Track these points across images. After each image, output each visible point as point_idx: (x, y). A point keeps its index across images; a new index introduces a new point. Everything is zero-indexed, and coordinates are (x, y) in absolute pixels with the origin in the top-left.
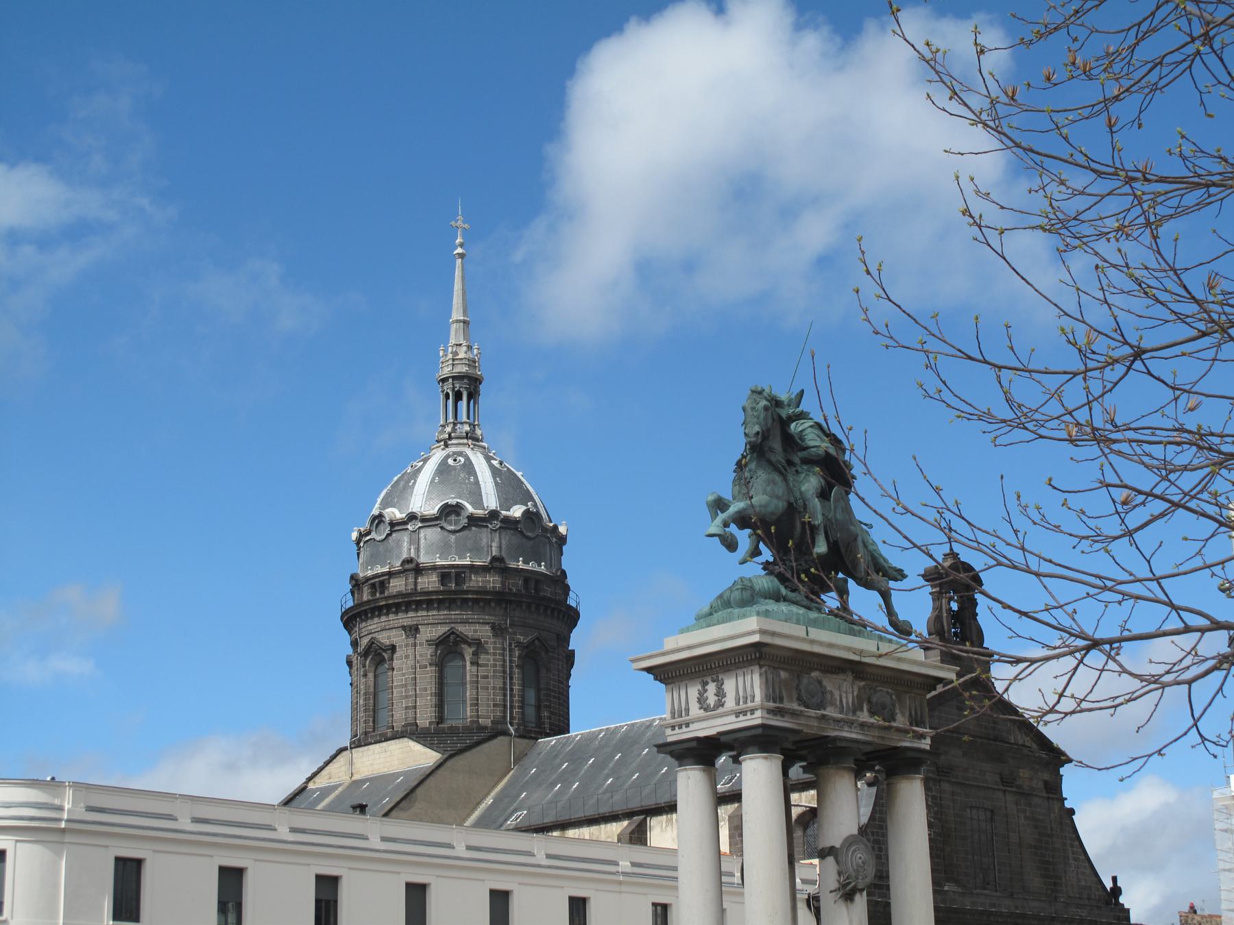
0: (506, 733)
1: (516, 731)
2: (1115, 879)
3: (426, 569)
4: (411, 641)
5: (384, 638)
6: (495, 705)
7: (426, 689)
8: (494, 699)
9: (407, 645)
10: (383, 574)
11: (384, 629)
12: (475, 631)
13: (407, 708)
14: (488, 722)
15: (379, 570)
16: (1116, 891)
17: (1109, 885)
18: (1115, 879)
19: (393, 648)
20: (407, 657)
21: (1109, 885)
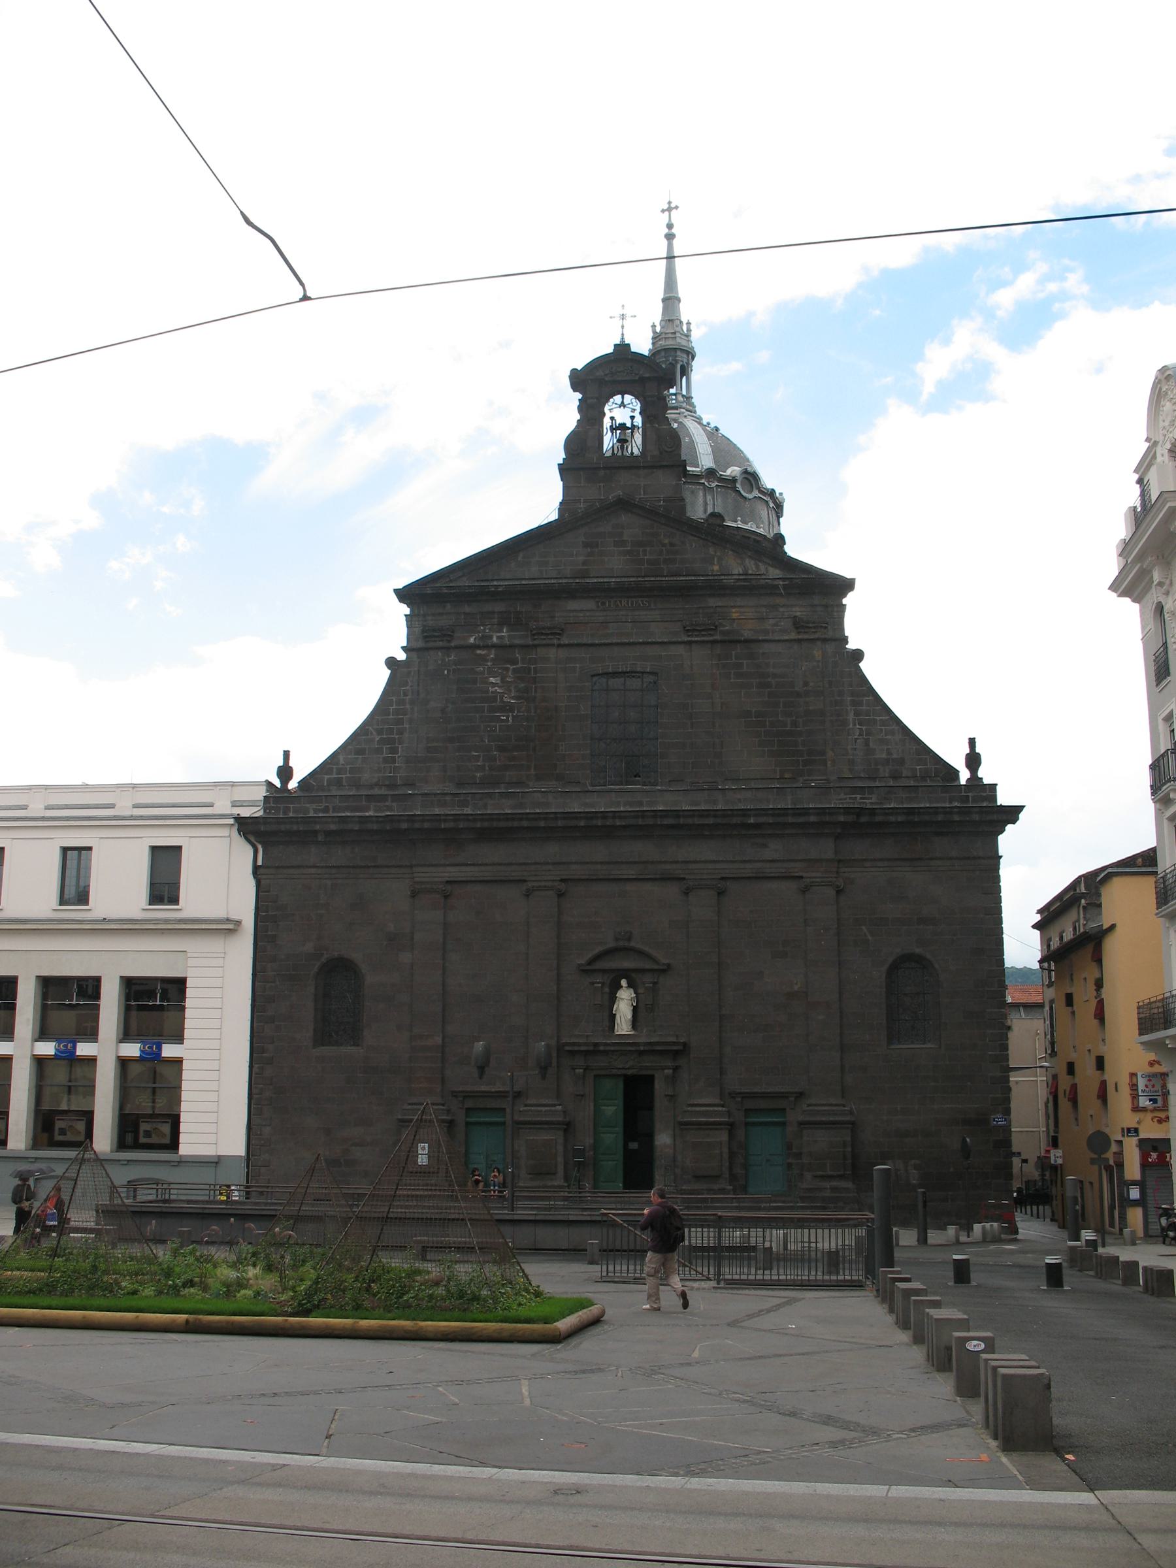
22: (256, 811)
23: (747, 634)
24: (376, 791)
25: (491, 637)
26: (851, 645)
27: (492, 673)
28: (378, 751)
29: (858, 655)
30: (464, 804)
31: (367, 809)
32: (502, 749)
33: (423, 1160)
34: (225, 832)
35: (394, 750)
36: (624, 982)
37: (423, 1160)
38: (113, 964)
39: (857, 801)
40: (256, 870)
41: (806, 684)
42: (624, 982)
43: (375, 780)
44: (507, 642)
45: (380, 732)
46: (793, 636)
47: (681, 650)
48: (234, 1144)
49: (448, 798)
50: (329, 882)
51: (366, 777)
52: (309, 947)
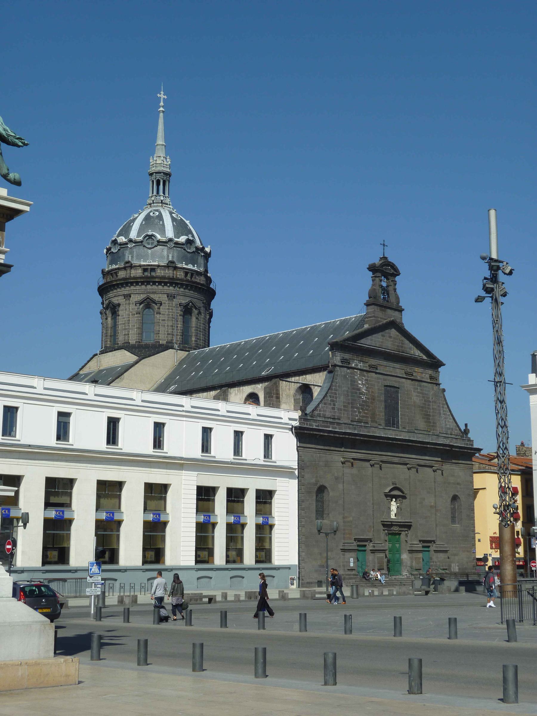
0: (172, 348)
1: (178, 347)
2: (466, 425)
3: (135, 266)
4: (128, 302)
5: (115, 301)
6: (168, 334)
7: (134, 326)
8: (167, 331)
9: (126, 304)
10: (116, 269)
11: (116, 296)
12: (160, 297)
13: (125, 335)
14: (165, 342)
15: (114, 267)
16: (466, 432)
17: (463, 428)
18: (466, 425)
19: (119, 305)
20: (126, 309)
21: (463, 428)
22: (296, 424)
23: (419, 378)
24: (330, 420)
25: (358, 365)
26: (442, 387)
27: (360, 380)
28: (330, 404)
29: (444, 390)
30: (355, 429)
31: (329, 427)
32: (362, 409)
33: (352, 565)
34: (288, 431)
35: (334, 405)
36: (394, 500)
37: (352, 565)
38: (252, 484)
39: (447, 442)
40: (297, 447)
41: (432, 398)
42: (394, 500)
43: (329, 416)
44: (362, 368)
45: (330, 396)
46: (429, 381)
47: (404, 380)
48: (293, 559)
49: (351, 426)
50: (318, 455)
51: (328, 414)
52: (313, 480)
